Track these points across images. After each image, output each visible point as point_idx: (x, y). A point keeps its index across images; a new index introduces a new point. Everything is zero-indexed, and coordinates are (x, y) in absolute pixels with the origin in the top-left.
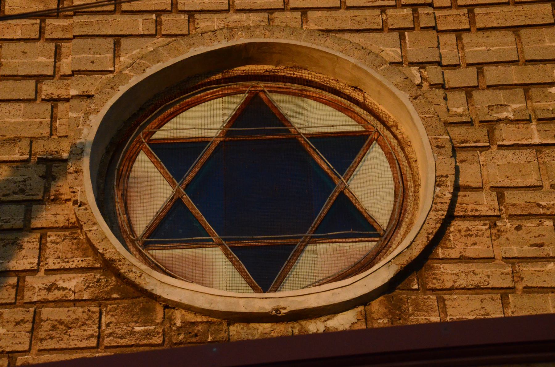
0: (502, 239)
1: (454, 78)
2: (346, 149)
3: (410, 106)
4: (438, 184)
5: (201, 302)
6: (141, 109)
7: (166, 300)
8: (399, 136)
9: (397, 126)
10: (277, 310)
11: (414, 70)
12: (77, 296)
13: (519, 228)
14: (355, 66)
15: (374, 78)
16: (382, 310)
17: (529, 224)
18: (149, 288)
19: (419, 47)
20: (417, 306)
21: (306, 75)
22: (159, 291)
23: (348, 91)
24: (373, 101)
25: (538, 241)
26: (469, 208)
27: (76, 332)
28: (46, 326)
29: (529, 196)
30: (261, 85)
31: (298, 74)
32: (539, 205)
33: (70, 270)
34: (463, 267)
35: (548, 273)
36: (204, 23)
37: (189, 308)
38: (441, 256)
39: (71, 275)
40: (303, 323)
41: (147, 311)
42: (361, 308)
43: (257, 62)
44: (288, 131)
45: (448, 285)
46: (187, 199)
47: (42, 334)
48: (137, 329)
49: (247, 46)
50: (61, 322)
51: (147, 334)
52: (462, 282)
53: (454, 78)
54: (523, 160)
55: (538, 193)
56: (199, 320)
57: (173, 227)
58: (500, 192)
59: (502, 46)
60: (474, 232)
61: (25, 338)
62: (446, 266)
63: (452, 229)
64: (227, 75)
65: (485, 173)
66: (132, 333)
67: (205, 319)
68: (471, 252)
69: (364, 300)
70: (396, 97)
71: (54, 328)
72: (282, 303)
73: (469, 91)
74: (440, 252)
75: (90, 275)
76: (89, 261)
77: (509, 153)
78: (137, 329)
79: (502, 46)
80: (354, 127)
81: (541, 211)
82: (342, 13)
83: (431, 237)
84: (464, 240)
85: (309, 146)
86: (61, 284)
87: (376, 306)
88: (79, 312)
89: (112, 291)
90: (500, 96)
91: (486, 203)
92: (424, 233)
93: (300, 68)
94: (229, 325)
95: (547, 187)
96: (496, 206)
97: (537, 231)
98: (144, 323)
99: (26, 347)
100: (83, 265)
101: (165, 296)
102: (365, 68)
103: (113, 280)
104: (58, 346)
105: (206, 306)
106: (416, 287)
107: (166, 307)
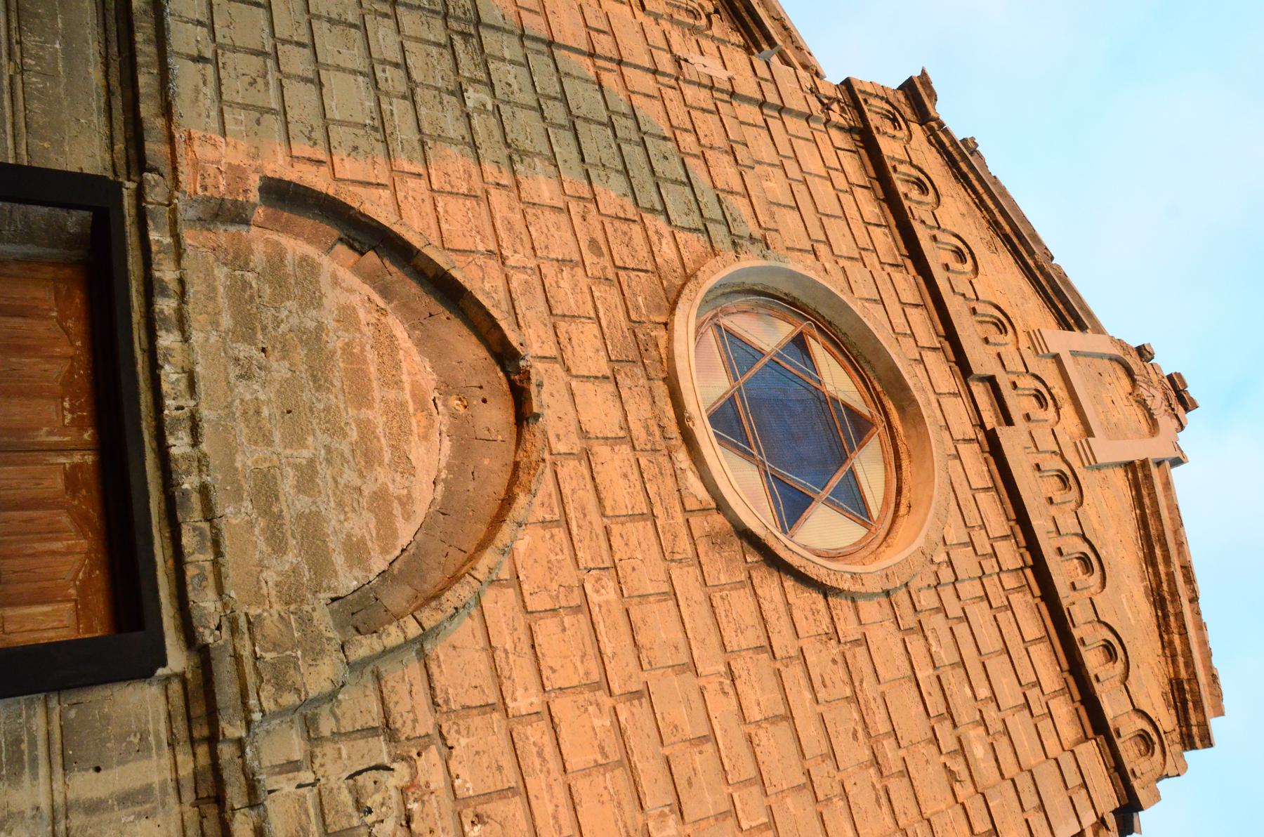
0: (819, 646)
1: (948, 593)
2: (852, 501)
3: (914, 547)
4: (853, 575)
5: (679, 348)
6: (830, 323)
7: (672, 321)
8: (881, 549)
9: (889, 546)
10: (689, 418)
11: (943, 557)
12: (656, 252)
13: (834, 662)
14: (931, 498)
15: (926, 515)
16: (718, 526)
17: (841, 673)
18: (680, 304)
19: (965, 562)
20: (730, 561)
21: (905, 463)
22: (679, 312)
23: (904, 501)
24: (903, 523)
25: (828, 682)
26: (839, 612)
27: (625, 251)
28: (625, 227)
29: (868, 670)
30: (881, 428)
31: (904, 456)
32: (861, 682)
33: (679, 250)
34: (782, 608)
35: (799, 692)
36: (919, 369)
37: (670, 340)
38: (785, 584)
39: (674, 249)
40: (684, 448)
41: (659, 308)
42: (714, 505)
43: (902, 419)
44: (852, 450)
45: (759, 591)
46: (766, 359)
47: (617, 223)
48: (640, 299)
49: (914, 401)
50: (630, 239)
51: (637, 308)
52: (766, 606)
53: (948, 593)
54: (898, 663)
55: (873, 679)
56: (662, 351)
57: (739, 352)
58: (864, 641)
59: (990, 642)
60: (818, 618)
61: (611, 211)
62: (777, 589)
63: (814, 595)
64: (882, 395)
65: (875, 626)
66: (635, 295)
67: (664, 356)
68: (797, 615)
69: (721, 506)
70: (917, 535)
71: (625, 233)
72: (698, 422)
73: (941, 609)
74: (789, 583)
75: (677, 264)
76: (690, 266)
77: (902, 650)
78: (640, 299)
79: (990, 642)
80: (875, 513)
81: (857, 684)
82: (969, 493)
83: (802, 570)
84: (808, 608)
85: (846, 468)
86: (664, 241)
87: (719, 520)
88: (643, 253)
89: (668, 281)
90: (947, 639)
91: (849, 629)
92: (804, 563)
93: (910, 456)
94: (664, 379)
95: (881, 688)
96: (849, 639)
97: (837, 681)
98: (647, 306)
99: (602, 211)
100: (686, 260)
101: (676, 318)
102: (933, 505)
103: (679, 282)
104: (609, 235)
105: (677, 353)
106: (749, 560)
107: (666, 324)
